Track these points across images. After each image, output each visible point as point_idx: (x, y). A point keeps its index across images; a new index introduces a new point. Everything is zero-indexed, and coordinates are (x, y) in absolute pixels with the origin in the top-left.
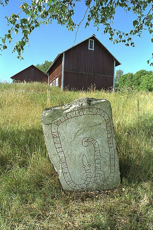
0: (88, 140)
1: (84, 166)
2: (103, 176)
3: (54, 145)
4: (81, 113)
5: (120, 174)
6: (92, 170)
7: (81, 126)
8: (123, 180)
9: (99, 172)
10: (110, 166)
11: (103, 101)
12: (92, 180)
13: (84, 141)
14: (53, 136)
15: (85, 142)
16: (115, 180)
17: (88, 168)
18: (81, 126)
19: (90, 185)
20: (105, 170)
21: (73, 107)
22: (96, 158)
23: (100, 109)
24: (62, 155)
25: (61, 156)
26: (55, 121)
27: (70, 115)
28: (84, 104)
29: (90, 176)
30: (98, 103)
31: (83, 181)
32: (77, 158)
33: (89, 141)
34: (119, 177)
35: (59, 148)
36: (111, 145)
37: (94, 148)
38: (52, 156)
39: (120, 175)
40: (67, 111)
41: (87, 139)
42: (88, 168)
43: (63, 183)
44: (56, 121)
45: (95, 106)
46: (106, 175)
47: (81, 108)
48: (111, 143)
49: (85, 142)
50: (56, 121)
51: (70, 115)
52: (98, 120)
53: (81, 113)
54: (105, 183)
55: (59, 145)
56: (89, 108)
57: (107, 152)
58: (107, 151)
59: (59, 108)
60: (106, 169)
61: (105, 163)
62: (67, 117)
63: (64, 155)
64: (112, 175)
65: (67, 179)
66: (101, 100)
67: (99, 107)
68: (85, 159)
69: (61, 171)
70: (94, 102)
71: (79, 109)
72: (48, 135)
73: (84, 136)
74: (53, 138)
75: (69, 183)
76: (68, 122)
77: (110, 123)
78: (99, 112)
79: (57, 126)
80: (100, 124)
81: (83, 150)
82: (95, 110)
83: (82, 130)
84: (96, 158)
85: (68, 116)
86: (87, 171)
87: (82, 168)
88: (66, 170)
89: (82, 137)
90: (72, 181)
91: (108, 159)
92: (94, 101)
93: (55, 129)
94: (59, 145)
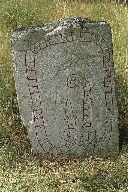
0: (76, 77)
1: (66, 118)
2: (93, 136)
3: (27, 82)
4: (70, 38)
5: (119, 134)
6: (79, 125)
7: (68, 56)
8: (123, 146)
9: (88, 129)
10: (105, 121)
11: (101, 23)
12: (77, 142)
13: (70, 79)
14: (26, 69)
15: (71, 80)
16: (111, 143)
17: (73, 121)
18: (68, 56)
19: (74, 149)
20: (98, 126)
21: (59, 28)
22: (85, 107)
23: (95, 35)
24: (36, 98)
25: (35, 99)
26: (31, 47)
27: (54, 40)
28: (74, 27)
29: (74, 134)
30: (94, 26)
31: (64, 142)
32: (57, 105)
33: (78, 80)
34: (118, 139)
35: (33, 87)
36: (108, 90)
37: (83, 91)
38: (22, 99)
39: (119, 137)
40: (49, 34)
41: (75, 76)
42: (73, 121)
43: (34, 142)
44: (33, 47)
45: (90, 30)
46: (99, 135)
47: (70, 31)
48: (108, 86)
49: (71, 80)
50: (33, 47)
51: (54, 40)
52: (92, 49)
53: (70, 38)
54: (96, 148)
55: (34, 83)
56: (81, 32)
57: (102, 99)
58: (103, 97)
59: (38, 29)
60: (99, 125)
61: (98, 115)
62: (50, 42)
63: (39, 98)
64: (107, 135)
65: (40, 137)
66: (99, 23)
67: (94, 32)
68: (69, 108)
69: (32, 122)
70: (86, 25)
71: (67, 32)
72: (20, 66)
73: (71, 72)
74: (27, 70)
75: (42, 142)
76: (50, 49)
77: (108, 56)
78: (94, 39)
79: (33, 54)
80: (94, 56)
81: (67, 92)
82: (88, 36)
83: (69, 63)
84: (85, 107)
85: (51, 41)
86: (71, 126)
87: (64, 120)
88: (40, 122)
89: (67, 72)
90: (47, 140)
91: (102, 110)
92: (89, 23)
93: (31, 58)
94: (34, 83)
